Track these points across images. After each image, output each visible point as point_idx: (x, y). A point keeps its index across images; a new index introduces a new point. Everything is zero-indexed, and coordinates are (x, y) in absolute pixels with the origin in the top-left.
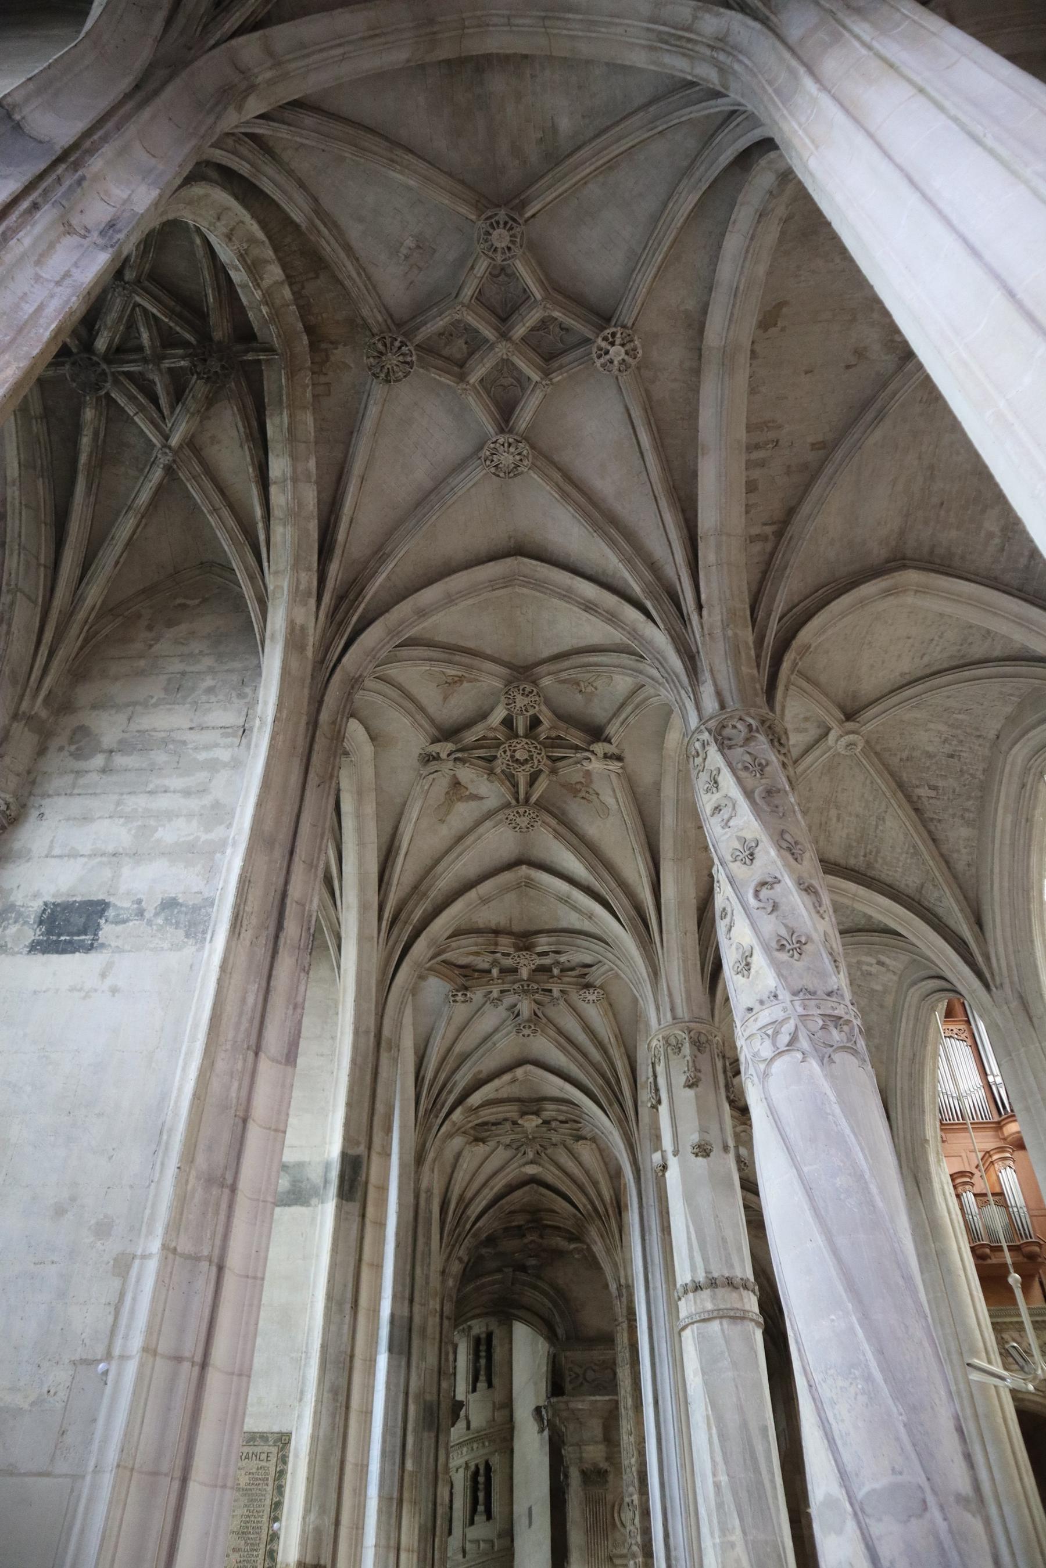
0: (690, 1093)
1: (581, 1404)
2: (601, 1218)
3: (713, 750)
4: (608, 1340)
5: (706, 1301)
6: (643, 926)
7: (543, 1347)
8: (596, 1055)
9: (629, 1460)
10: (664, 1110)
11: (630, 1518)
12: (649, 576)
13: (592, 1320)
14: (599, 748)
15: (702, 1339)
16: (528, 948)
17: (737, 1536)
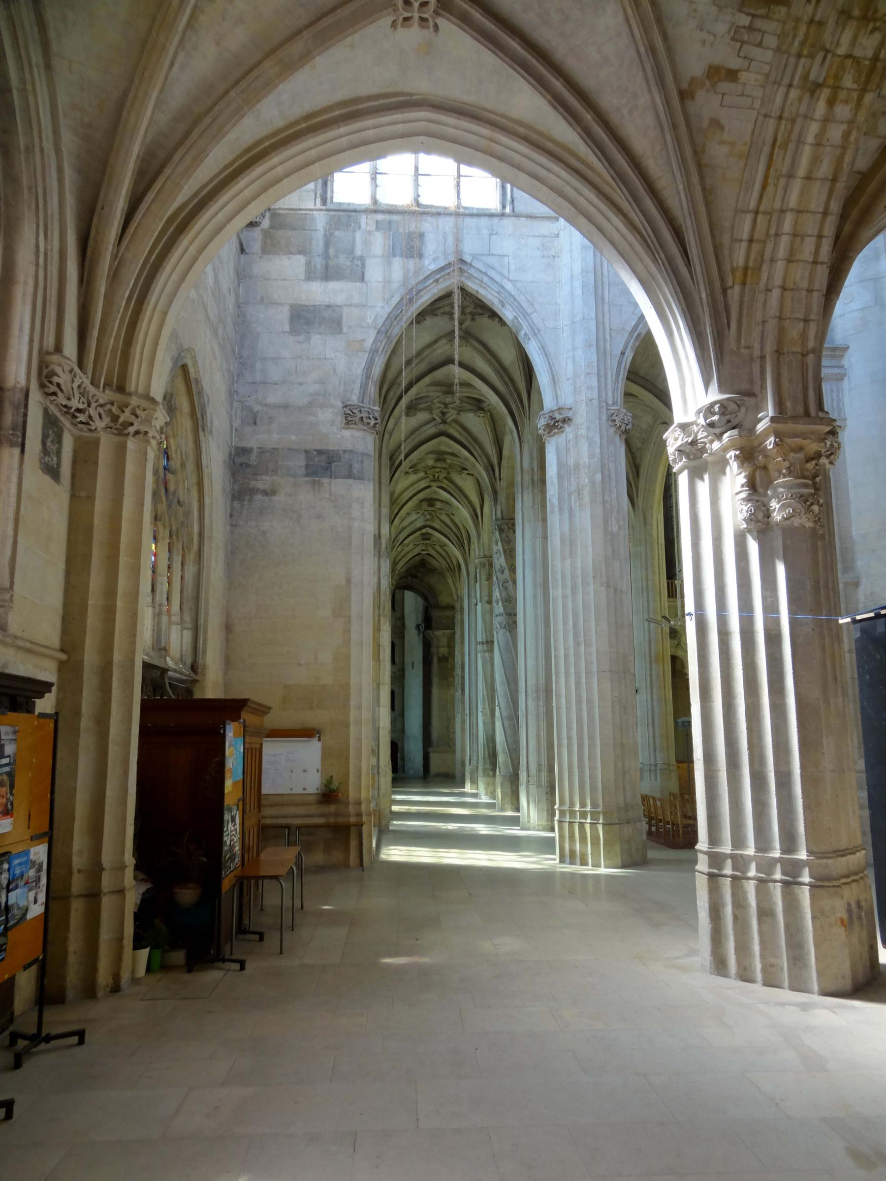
0: (487, 583)
1: (439, 633)
2: (450, 569)
3: (497, 533)
4: (452, 608)
5: (485, 647)
6: (475, 516)
7: (420, 600)
8: (454, 529)
9: (458, 659)
10: (478, 585)
11: (458, 680)
12: (485, 461)
13: (444, 600)
14: (466, 472)
15: (483, 658)
16: (432, 505)
17: (487, 706)
